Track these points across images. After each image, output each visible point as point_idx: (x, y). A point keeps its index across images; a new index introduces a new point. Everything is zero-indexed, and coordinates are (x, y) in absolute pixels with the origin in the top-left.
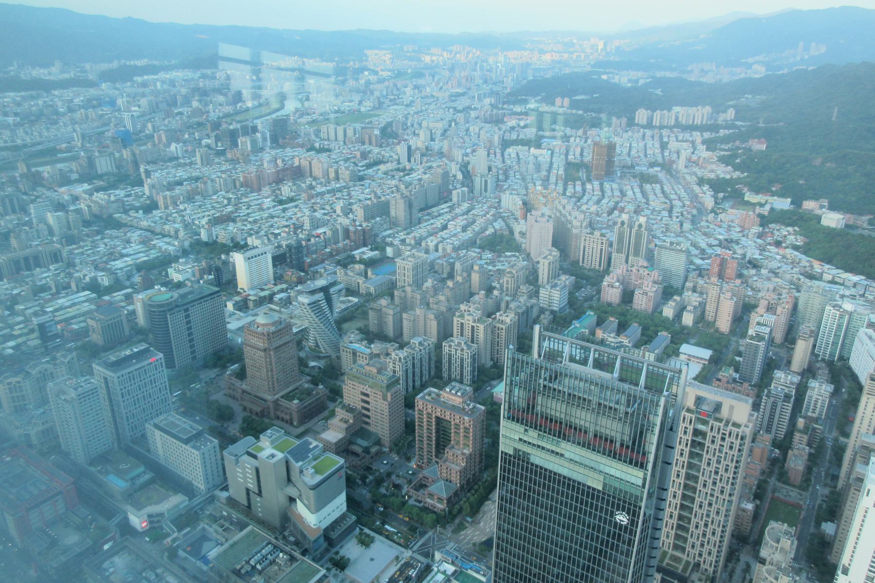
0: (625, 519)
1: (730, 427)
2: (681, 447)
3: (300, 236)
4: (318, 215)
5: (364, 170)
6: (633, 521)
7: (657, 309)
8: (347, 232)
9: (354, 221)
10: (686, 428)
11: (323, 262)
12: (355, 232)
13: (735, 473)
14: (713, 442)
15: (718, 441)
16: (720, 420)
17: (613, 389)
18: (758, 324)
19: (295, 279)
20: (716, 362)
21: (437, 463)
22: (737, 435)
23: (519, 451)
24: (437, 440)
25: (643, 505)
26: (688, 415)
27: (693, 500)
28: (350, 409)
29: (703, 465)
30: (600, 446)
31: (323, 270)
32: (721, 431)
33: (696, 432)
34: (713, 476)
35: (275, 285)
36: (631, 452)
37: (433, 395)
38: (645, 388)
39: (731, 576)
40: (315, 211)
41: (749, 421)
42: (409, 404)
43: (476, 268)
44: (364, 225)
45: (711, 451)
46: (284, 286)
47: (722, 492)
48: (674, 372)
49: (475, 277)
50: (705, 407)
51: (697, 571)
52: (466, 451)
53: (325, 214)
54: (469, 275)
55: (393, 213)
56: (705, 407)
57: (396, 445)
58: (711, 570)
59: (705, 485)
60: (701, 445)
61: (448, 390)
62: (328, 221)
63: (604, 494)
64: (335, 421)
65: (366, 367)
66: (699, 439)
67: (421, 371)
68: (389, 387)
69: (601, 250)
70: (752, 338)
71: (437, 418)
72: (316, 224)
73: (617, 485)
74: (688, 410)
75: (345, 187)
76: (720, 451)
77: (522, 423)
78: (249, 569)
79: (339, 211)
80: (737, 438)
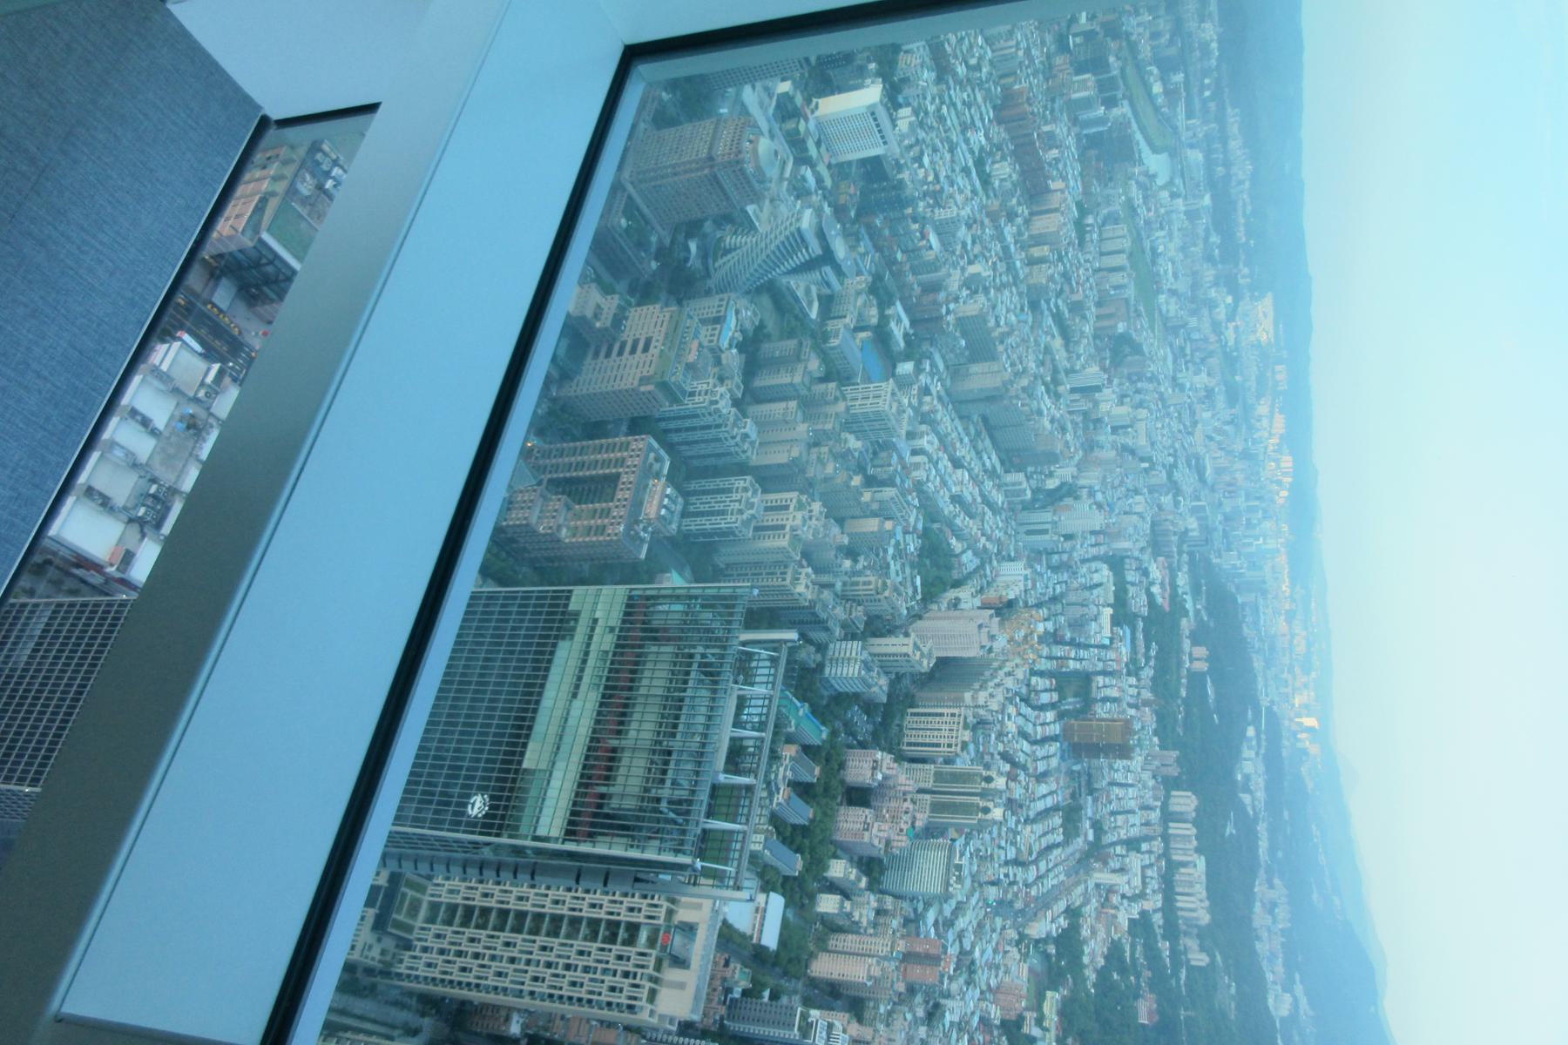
0: (476, 810)
1: (648, 985)
2: (605, 904)
3: (921, 204)
4: (962, 232)
5: (1049, 309)
6: (475, 825)
7: (842, 849)
8: (933, 288)
9: (956, 300)
10: (640, 910)
11: (878, 248)
12: (935, 302)
13: (570, 998)
14: (620, 958)
15: (621, 967)
16: (658, 966)
17: (697, 773)
18: (830, 1026)
19: (842, 199)
20: (759, 956)
21: (540, 483)
22: (635, 999)
23: (576, 621)
24: (579, 480)
25: (504, 840)
26: (662, 913)
27: (517, 929)
28: (619, 320)
29: (578, 944)
30: (597, 758)
31: (862, 250)
32: (640, 971)
33: (633, 928)
34: (562, 961)
35: (829, 166)
36: (591, 814)
37: (656, 466)
38: (704, 831)
39: (396, 1004)
40: (969, 227)
41: (662, 1017)
42: (637, 425)
43: (888, 525)
44: (950, 318)
45: (604, 956)
46: (828, 183)
47: (536, 979)
48: (736, 879)
49: (872, 525)
50: (678, 940)
51: (397, 946)
52: (564, 531)
53: (964, 245)
54: (874, 514)
55: (975, 368)
56: (678, 940)
57: (563, 409)
58: (402, 969)
59: (544, 948)
60: (612, 939)
61: (669, 491)
62: (953, 253)
63: (517, 772)
64: (596, 296)
65: (695, 343)
66: (622, 934)
67: (696, 442)
68: (664, 386)
69: (938, 745)
70: (804, 1016)
71: (618, 475)
72: (945, 231)
73: (533, 793)
74: (670, 913)
75: (1016, 277)
76: (605, 971)
77: (624, 622)
78: (325, 168)
79: (972, 269)
80: (630, 998)
